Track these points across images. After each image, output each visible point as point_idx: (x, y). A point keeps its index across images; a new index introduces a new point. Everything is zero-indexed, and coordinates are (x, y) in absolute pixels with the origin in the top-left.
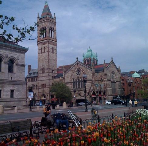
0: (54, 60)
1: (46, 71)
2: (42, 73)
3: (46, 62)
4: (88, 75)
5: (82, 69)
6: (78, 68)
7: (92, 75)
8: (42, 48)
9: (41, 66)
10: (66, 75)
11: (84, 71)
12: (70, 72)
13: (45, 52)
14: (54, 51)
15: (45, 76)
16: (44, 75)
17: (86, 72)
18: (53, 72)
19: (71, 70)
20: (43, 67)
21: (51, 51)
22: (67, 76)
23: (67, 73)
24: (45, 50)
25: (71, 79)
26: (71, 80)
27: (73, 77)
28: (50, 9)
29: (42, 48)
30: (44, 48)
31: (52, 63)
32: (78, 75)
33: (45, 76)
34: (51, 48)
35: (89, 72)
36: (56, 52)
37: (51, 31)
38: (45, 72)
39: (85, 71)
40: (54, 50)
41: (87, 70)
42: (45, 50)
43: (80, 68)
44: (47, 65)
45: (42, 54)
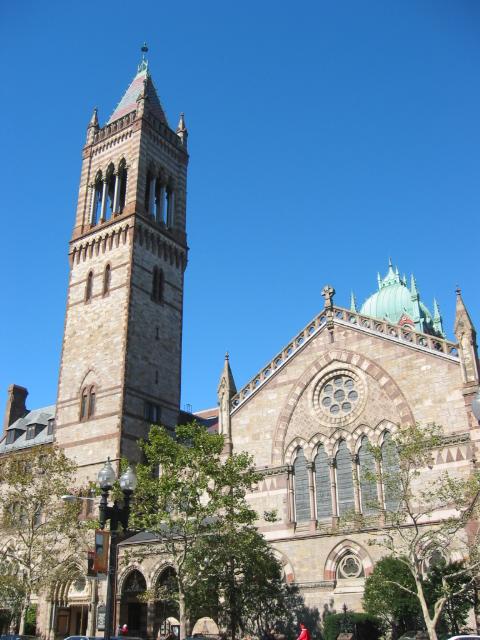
0: (164, 346)
1: (101, 407)
2: (77, 419)
3: (106, 348)
4: (428, 403)
5: (374, 364)
6: (333, 356)
7: (458, 395)
8: (96, 272)
9: (79, 375)
10: (242, 420)
11: (383, 373)
12: (270, 395)
13: (106, 291)
14: (168, 294)
15: (98, 439)
16: (93, 428)
17: (402, 383)
18: (150, 413)
19: (280, 379)
20: (88, 382)
21: (150, 287)
22: (248, 427)
23: (250, 405)
24: (107, 281)
25: (275, 444)
26: (284, 455)
27: (293, 431)
28: (158, 93)
29: (91, 274)
30: (108, 267)
31: (145, 358)
32: (334, 408)
33: (98, 439)
34: (151, 270)
35: (428, 382)
36: (177, 305)
37: (154, 184)
38: (97, 414)
39: (393, 371)
40: (166, 285)
41: (410, 367)
42: (107, 281)
43: (351, 355)
44: (112, 369)
45: (87, 308)
